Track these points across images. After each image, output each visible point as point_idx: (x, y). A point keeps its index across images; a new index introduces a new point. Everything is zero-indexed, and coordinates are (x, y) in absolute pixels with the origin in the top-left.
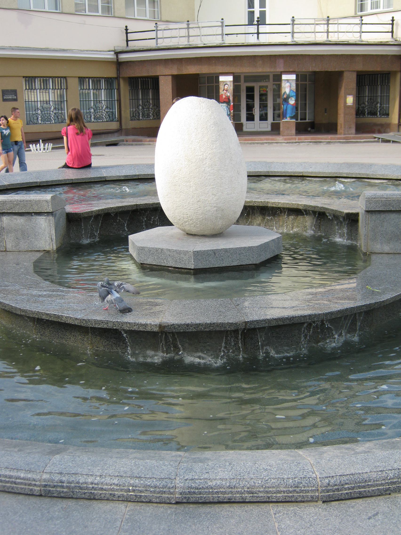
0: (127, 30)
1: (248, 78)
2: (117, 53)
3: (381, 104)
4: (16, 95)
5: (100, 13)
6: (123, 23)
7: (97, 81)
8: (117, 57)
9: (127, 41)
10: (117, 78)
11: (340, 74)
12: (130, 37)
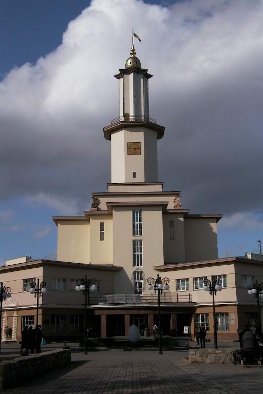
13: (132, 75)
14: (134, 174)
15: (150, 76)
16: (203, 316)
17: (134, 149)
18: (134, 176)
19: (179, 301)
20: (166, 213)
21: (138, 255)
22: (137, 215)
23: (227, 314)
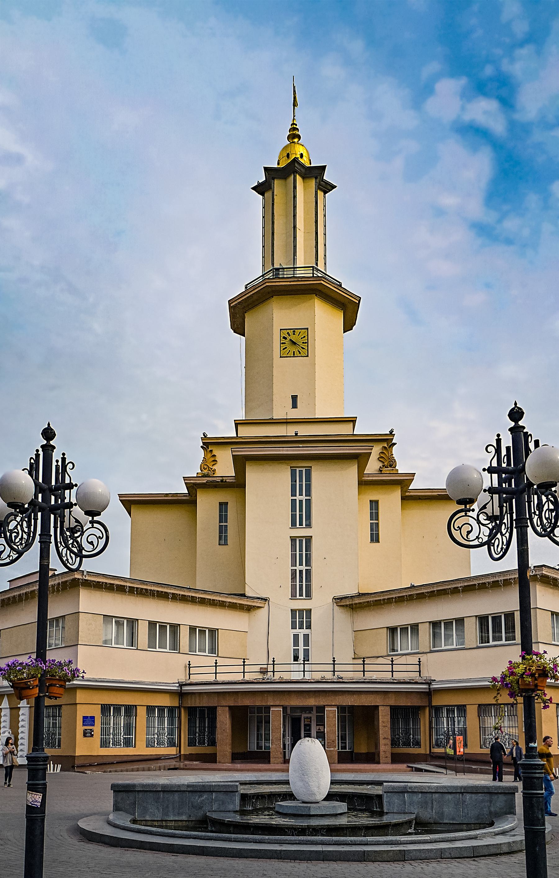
0: (189, 665)
1: (294, 709)
2: (181, 685)
3: (413, 736)
7: (161, 709)
8: (181, 688)
10: (179, 708)
11: (377, 707)
15: (327, 187)
17: (294, 343)
19: (397, 676)
20: (364, 484)
21: (301, 494)
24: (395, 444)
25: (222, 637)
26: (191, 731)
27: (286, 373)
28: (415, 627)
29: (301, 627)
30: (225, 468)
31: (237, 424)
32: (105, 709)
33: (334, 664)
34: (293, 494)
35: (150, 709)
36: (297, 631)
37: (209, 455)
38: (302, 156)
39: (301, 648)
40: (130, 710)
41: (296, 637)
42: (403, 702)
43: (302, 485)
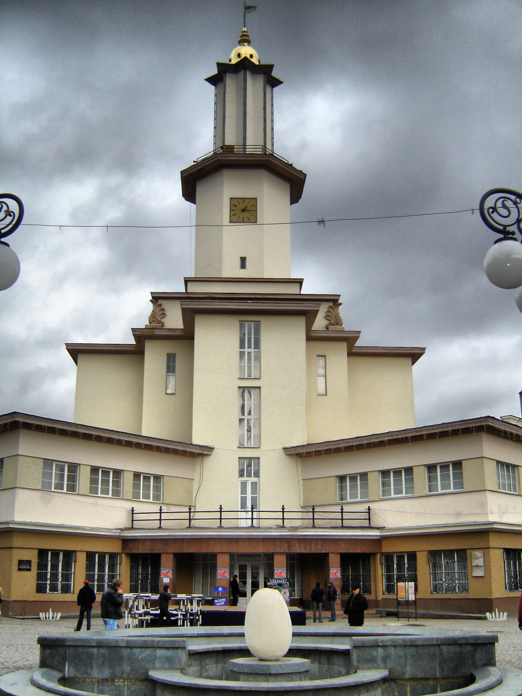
0: (133, 511)
3: (363, 582)
4: (30, 566)
5: (110, 496)
6: (129, 505)
7: (102, 556)
9: (133, 520)
11: (326, 555)
12: (136, 517)
13: (242, 73)
14: (243, 260)
15: (274, 83)
16: (400, 558)
18: (243, 265)
20: (311, 338)
22: (250, 334)
23: (463, 554)
24: (341, 304)
25: (166, 484)
26: (133, 578)
27: (235, 239)
28: (364, 476)
29: (249, 475)
30: (174, 320)
31: (187, 281)
32: (42, 553)
33: (283, 512)
34: (242, 346)
35: (90, 556)
36: (245, 479)
37: (159, 309)
38: (251, 56)
39: (249, 496)
40: (69, 555)
41: (244, 485)
42: (352, 550)
43: (250, 343)
